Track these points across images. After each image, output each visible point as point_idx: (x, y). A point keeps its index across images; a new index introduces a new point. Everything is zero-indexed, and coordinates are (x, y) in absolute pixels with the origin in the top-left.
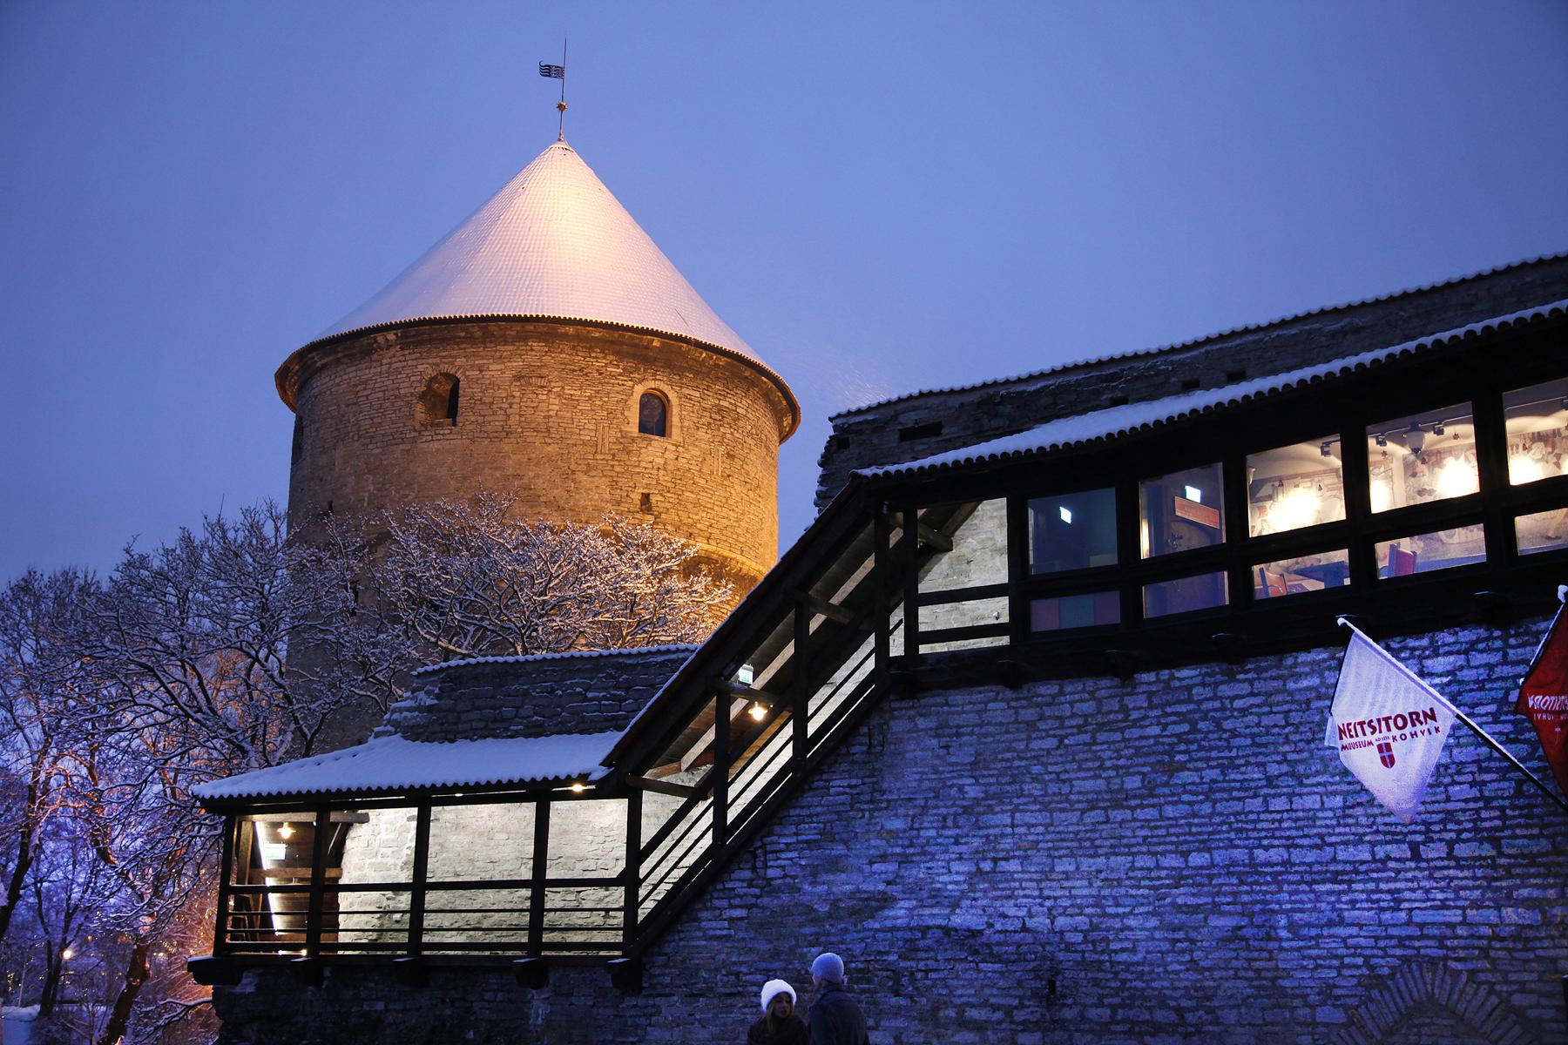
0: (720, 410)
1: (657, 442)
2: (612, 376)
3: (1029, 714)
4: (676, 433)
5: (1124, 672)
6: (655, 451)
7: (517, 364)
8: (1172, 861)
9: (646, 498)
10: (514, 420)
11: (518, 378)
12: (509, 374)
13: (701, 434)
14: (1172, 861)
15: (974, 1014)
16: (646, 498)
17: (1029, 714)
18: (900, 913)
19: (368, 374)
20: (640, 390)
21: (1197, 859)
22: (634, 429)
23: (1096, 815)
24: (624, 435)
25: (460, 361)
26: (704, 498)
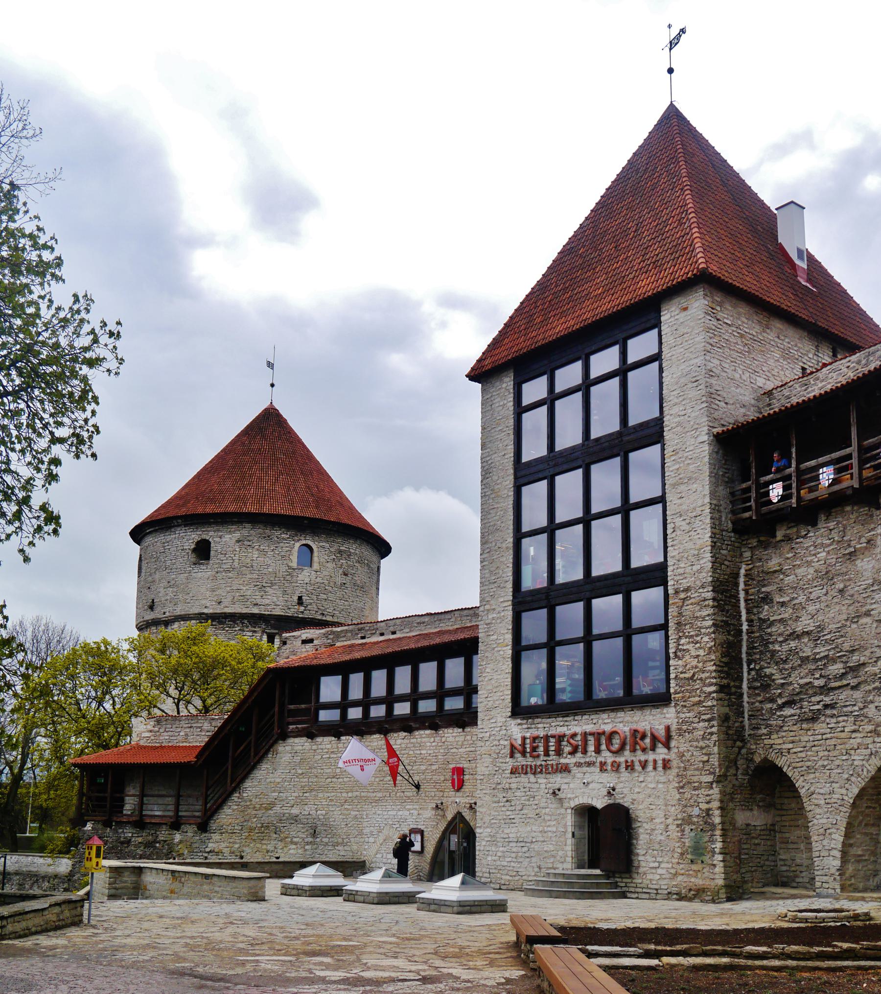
0: (340, 552)
1: (307, 572)
2: (284, 539)
3: (314, 747)
4: (316, 566)
5: (338, 735)
6: (305, 575)
7: (237, 535)
8: (344, 795)
9: (300, 598)
10: (236, 564)
11: (238, 541)
12: (234, 539)
13: (329, 565)
14: (344, 795)
15: (295, 840)
16: (300, 598)
17: (314, 747)
18: (277, 809)
19: (169, 538)
20: (298, 545)
21: (350, 795)
22: (294, 564)
23: (329, 780)
24: (290, 567)
25: (211, 533)
26: (331, 597)
